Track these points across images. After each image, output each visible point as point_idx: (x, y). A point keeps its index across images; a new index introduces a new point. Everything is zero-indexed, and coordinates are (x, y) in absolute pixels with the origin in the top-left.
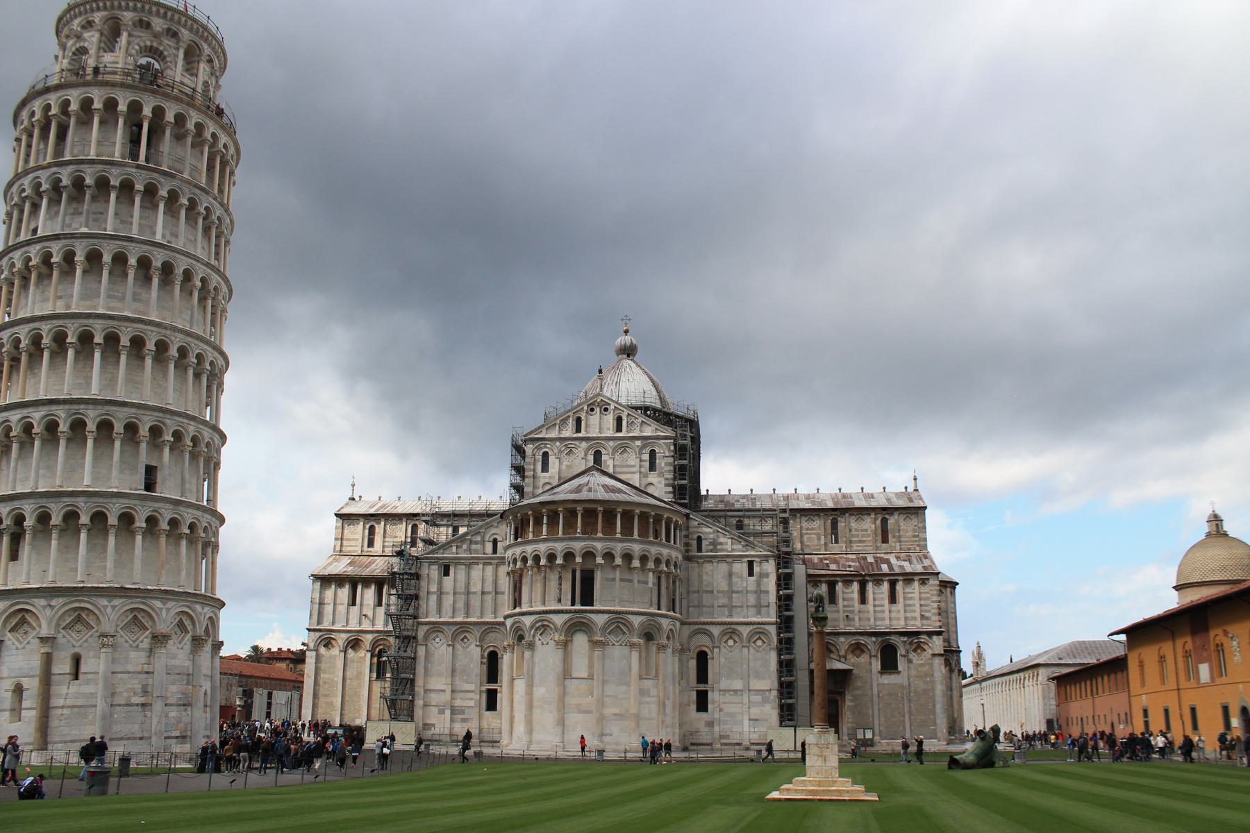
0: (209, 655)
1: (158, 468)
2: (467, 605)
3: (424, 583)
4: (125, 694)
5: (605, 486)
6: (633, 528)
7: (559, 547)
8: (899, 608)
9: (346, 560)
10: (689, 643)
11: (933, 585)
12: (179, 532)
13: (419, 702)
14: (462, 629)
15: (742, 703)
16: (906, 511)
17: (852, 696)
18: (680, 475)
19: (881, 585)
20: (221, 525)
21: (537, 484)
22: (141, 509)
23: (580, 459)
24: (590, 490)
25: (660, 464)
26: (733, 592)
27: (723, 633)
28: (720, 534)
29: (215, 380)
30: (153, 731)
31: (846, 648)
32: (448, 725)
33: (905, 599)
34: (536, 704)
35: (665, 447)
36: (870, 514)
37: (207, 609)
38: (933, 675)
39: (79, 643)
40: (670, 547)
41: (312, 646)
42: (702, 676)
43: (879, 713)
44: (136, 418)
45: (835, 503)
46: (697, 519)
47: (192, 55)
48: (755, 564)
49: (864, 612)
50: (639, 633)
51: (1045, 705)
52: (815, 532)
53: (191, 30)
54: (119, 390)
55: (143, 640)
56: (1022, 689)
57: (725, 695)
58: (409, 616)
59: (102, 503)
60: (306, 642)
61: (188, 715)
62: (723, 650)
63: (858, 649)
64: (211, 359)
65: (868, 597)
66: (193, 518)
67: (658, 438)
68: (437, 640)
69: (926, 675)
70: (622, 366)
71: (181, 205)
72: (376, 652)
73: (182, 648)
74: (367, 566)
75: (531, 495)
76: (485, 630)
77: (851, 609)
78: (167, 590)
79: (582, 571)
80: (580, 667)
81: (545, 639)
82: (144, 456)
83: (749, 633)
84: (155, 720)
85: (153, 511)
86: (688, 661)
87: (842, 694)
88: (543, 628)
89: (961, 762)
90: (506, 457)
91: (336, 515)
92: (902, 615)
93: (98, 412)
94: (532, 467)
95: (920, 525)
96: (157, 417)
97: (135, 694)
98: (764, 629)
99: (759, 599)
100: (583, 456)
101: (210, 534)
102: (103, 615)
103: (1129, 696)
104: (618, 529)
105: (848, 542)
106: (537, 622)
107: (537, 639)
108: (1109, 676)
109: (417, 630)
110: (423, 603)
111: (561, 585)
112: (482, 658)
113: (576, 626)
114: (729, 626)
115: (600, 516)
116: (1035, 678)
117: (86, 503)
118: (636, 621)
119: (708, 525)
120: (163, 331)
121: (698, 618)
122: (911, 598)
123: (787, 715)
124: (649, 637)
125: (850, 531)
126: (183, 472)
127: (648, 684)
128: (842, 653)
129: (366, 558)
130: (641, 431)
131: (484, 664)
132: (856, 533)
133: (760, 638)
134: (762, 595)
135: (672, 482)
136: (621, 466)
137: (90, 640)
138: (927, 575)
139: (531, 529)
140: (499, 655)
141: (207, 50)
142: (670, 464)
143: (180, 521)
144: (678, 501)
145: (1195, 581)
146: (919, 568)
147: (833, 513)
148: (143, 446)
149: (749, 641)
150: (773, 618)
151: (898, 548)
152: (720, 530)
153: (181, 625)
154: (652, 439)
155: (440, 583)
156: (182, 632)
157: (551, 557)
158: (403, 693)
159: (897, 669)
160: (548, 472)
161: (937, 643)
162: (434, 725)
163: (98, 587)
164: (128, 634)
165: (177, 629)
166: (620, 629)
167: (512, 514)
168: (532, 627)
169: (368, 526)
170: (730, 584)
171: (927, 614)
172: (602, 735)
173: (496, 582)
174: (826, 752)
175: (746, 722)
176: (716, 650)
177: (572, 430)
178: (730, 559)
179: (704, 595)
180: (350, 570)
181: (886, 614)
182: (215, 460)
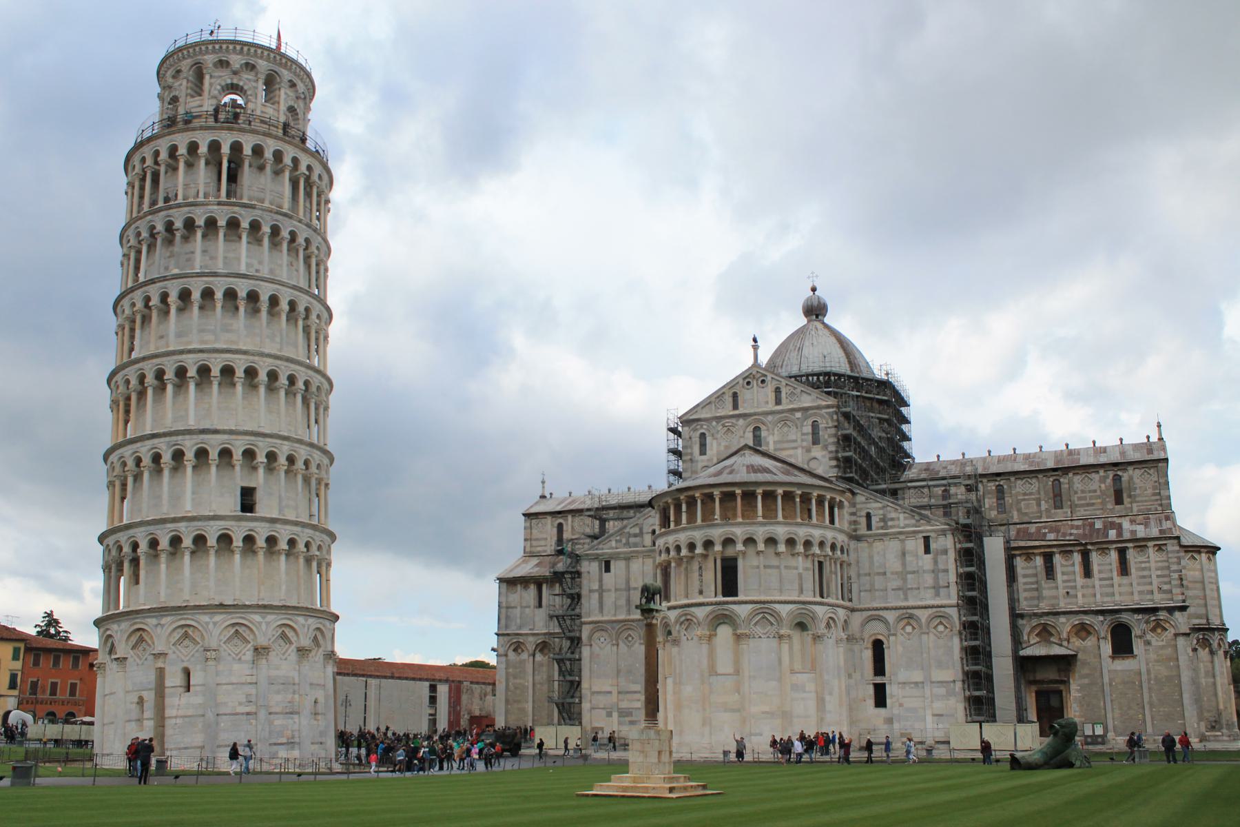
5: (753, 469)
7: (698, 536)
9: (535, 561)
10: (862, 631)
13: (586, 706)
17: (1079, 685)
27: (900, 619)
35: (827, 416)
36: (1098, 472)
37: (311, 621)
39: (188, 658)
41: (502, 651)
42: (879, 668)
43: (1112, 705)
44: (228, 444)
45: (1057, 462)
47: (270, 82)
52: (1033, 497)
53: (268, 59)
60: (496, 647)
61: (295, 722)
62: (900, 638)
63: (1083, 630)
67: (818, 408)
68: (602, 639)
69: (1169, 659)
71: (264, 234)
73: (286, 659)
79: (724, 560)
83: (928, 618)
85: (250, 530)
86: (861, 651)
87: (1066, 683)
88: (688, 622)
89: (1022, 761)
91: (524, 515)
93: (194, 442)
96: (248, 440)
97: (240, 704)
98: (945, 612)
99: (936, 579)
100: (742, 434)
104: (760, 512)
106: (681, 616)
109: (581, 631)
111: (701, 575)
114: (905, 611)
115: (739, 500)
117: (187, 527)
120: (251, 358)
122: (1144, 569)
133: (941, 623)
137: (197, 655)
141: (286, 75)
142: (835, 435)
146: (1155, 532)
153: (284, 636)
155: (601, 581)
159: (1133, 653)
160: (705, 454)
165: (281, 641)
166: (767, 619)
168: (676, 622)
169: (556, 525)
170: (904, 564)
175: (929, 718)
176: (892, 638)
178: (901, 535)
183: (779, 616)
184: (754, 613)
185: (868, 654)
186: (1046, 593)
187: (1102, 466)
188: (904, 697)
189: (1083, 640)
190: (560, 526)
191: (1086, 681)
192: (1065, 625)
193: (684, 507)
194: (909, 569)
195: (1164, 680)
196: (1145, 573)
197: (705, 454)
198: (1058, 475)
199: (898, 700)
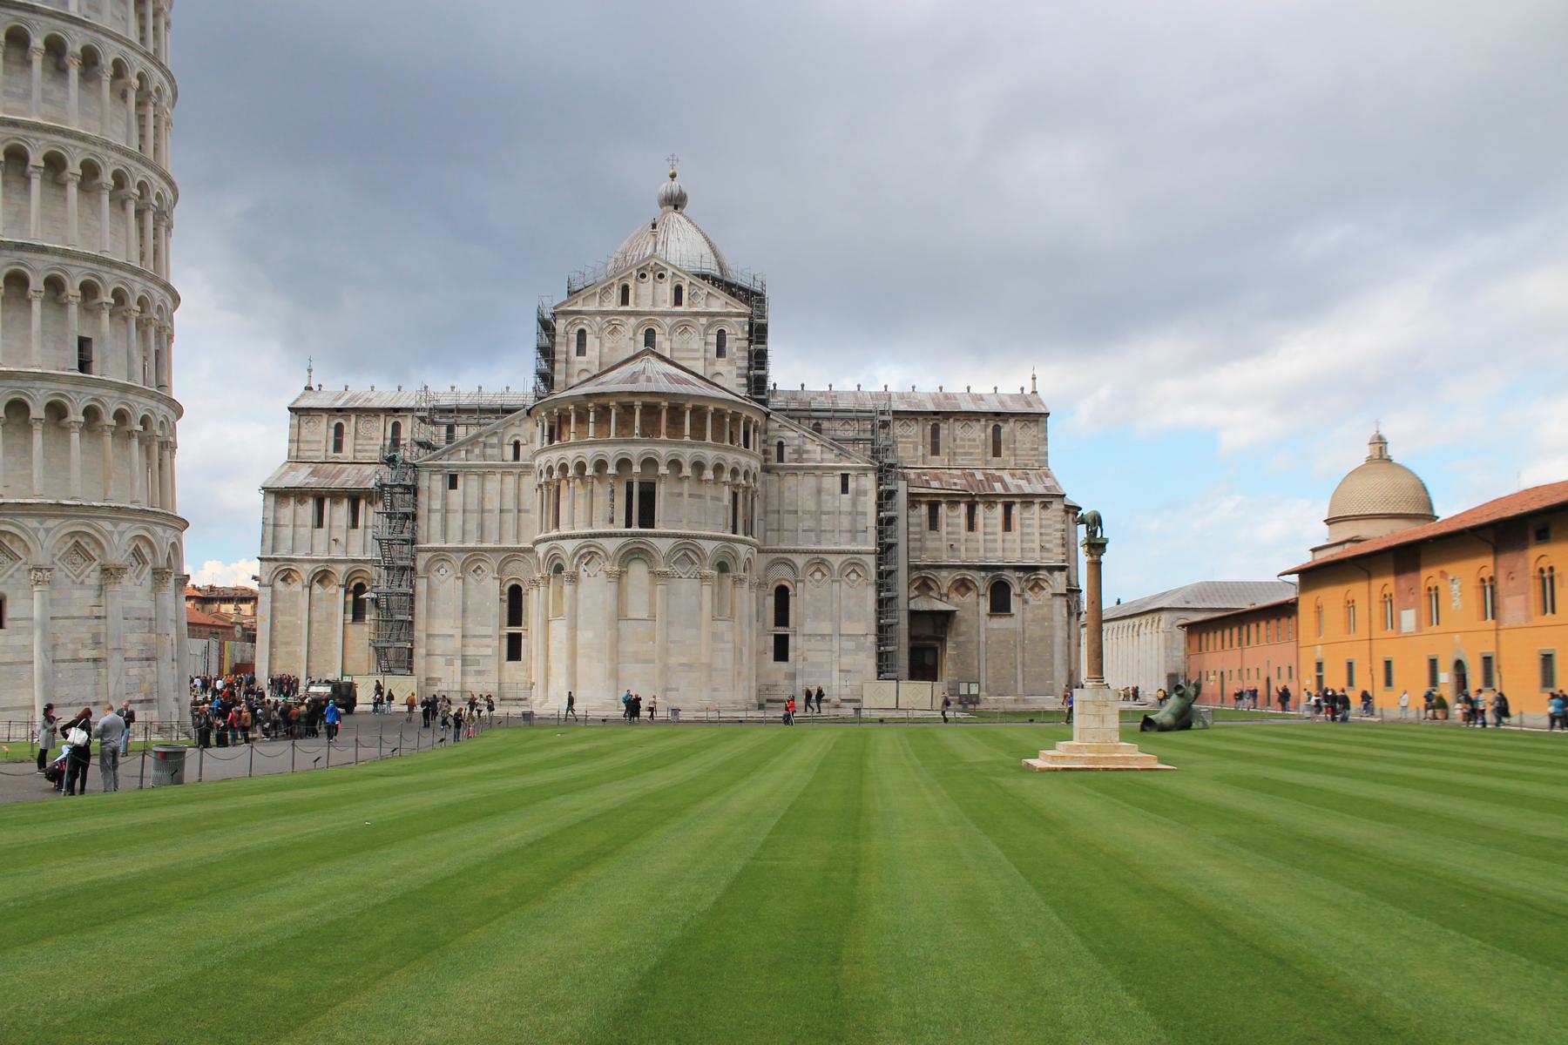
0: (172, 593)
1: (93, 341)
2: (482, 527)
3: (422, 498)
4: (70, 646)
6: (705, 430)
7: (611, 453)
8: (1015, 537)
9: (306, 469)
10: (766, 576)
11: (1057, 510)
12: (127, 428)
13: (420, 652)
14: (473, 559)
15: (831, 651)
16: (1025, 418)
18: (757, 363)
19: (993, 508)
20: (178, 418)
21: (570, 371)
22: (76, 396)
23: (628, 340)
24: (649, 379)
26: (822, 513)
27: (809, 564)
28: (808, 440)
29: (163, 220)
30: (111, 694)
31: (949, 585)
32: (458, 678)
33: (1022, 526)
34: (580, 651)
36: (979, 421)
37: (169, 532)
38: (1052, 619)
40: (750, 455)
41: (265, 580)
42: (782, 616)
44: (59, 270)
45: (937, 405)
46: (778, 420)
48: (850, 477)
49: (972, 540)
50: (712, 562)
51: (1167, 656)
54: (32, 232)
55: (89, 574)
56: (1136, 637)
57: (810, 641)
58: (403, 540)
59: (20, 388)
60: (257, 574)
61: (153, 672)
62: (808, 585)
63: (963, 585)
64: (158, 190)
66: (146, 410)
67: (729, 315)
68: (442, 571)
70: (669, 220)
72: (352, 588)
73: (140, 585)
74: (336, 476)
75: (563, 385)
76: (504, 559)
78: (119, 508)
79: (641, 484)
80: (638, 605)
81: (592, 569)
82: (75, 324)
83: (841, 565)
84: (112, 680)
85: (93, 399)
86: (764, 599)
87: (942, 640)
88: (589, 556)
89: (1158, 722)
90: (530, 336)
91: (289, 409)
92: (1017, 545)
94: (565, 349)
95: (1041, 436)
96: (90, 269)
97: (84, 646)
98: (860, 559)
99: (854, 522)
100: (631, 336)
101: (167, 432)
102: (34, 543)
103: (1297, 647)
104: (687, 431)
105: (952, 454)
106: (581, 549)
107: (581, 570)
108: (1268, 622)
110: (422, 523)
112: (501, 594)
113: (632, 554)
114: (816, 555)
116: (1155, 624)
118: (709, 547)
119: (793, 428)
120: (91, 147)
121: (778, 545)
122: (1029, 526)
123: (884, 665)
124: (722, 567)
125: (955, 440)
126: (128, 346)
127: (723, 626)
128: (944, 591)
129: (332, 466)
130: (707, 305)
131: (504, 601)
132: (962, 443)
133: (854, 571)
134: (859, 517)
135: (745, 372)
136: (678, 350)
137: (17, 575)
138: (1049, 498)
139: (572, 428)
140: (524, 591)
142: (744, 349)
143: (129, 414)
144: (755, 397)
145: (1352, 514)
146: (1042, 491)
147: (935, 417)
148: (73, 309)
149: (841, 575)
150: (872, 547)
152: (806, 434)
153: (137, 553)
154: (718, 316)
155: (445, 498)
156: (139, 564)
157: (601, 465)
158: (398, 640)
159: (1008, 609)
160: (584, 355)
161: (1059, 580)
162: (440, 679)
163: (25, 504)
164: (69, 566)
166: (689, 558)
167: (546, 410)
168: (575, 554)
169: (333, 424)
170: (819, 503)
171: (1047, 545)
172: (667, 690)
173: (518, 497)
174: (1105, 711)
175: (836, 674)
177: (617, 302)
180: (314, 482)
181: (999, 545)
182: (168, 330)
183: (703, 553)
184: (675, 550)
185: (771, 602)
186: (929, 544)
187: (985, 414)
188: (808, 650)
189: (963, 596)
190: (339, 429)
192: (946, 578)
193: (592, 418)
194: (825, 509)
196: (1029, 530)
197: (584, 355)
198: (938, 419)
199: (803, 653)
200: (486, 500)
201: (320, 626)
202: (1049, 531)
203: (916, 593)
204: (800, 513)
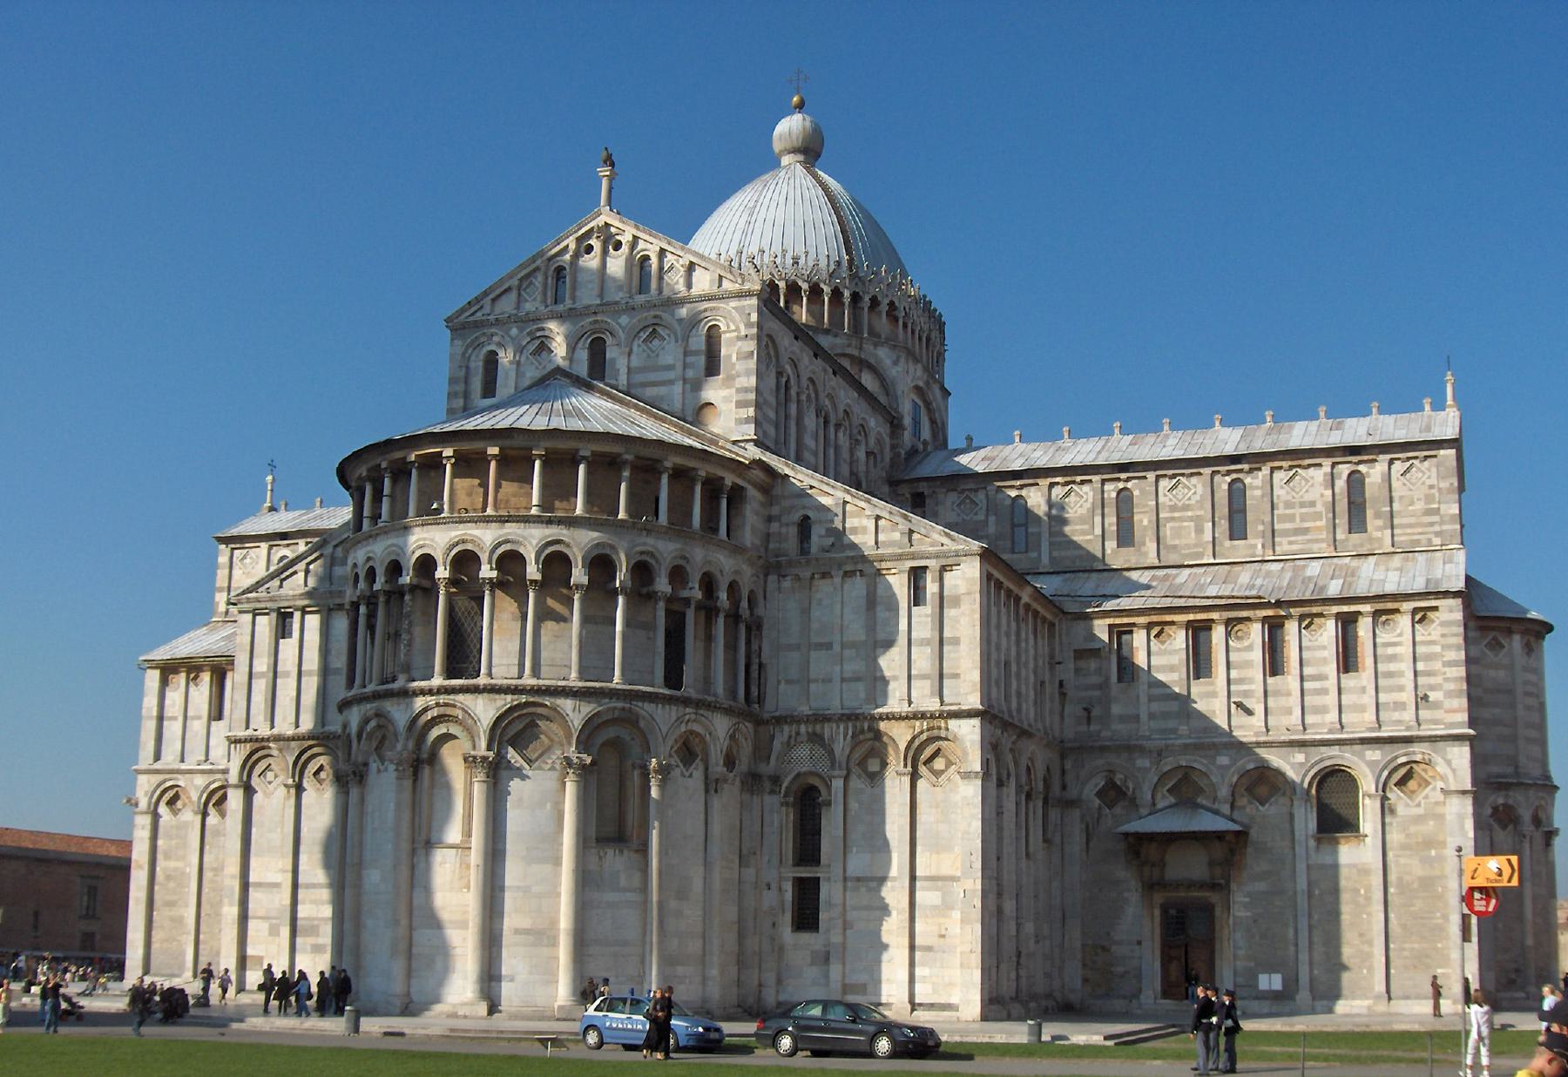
8: (1364, 683)
11: (1443, 624)
17: (1245, 897)
19: (1320, 627)
25: (729, 356)
48: (929, 577)
52: (1190, 514)
65: (1288, 657)
68: (270, 775)
69: (1429, 843)
77: (1245, 687)
87: (1220, 886)
92: (1368, 699)
105: (1269, 534)
122: (1393, 658)
132: (1288, 512)
136: (641, 370)
151: (1388, 541)
159: (1357, 830)
179: (813, 654)
189: (1262, 804)
191: (1261, 886)
195: (1415, 885)
198: (1240, 471)
200: (333, 652)
201: (215, 875)
202: (1437, 665)
203: (1172, 800)
204: (837, 648)
